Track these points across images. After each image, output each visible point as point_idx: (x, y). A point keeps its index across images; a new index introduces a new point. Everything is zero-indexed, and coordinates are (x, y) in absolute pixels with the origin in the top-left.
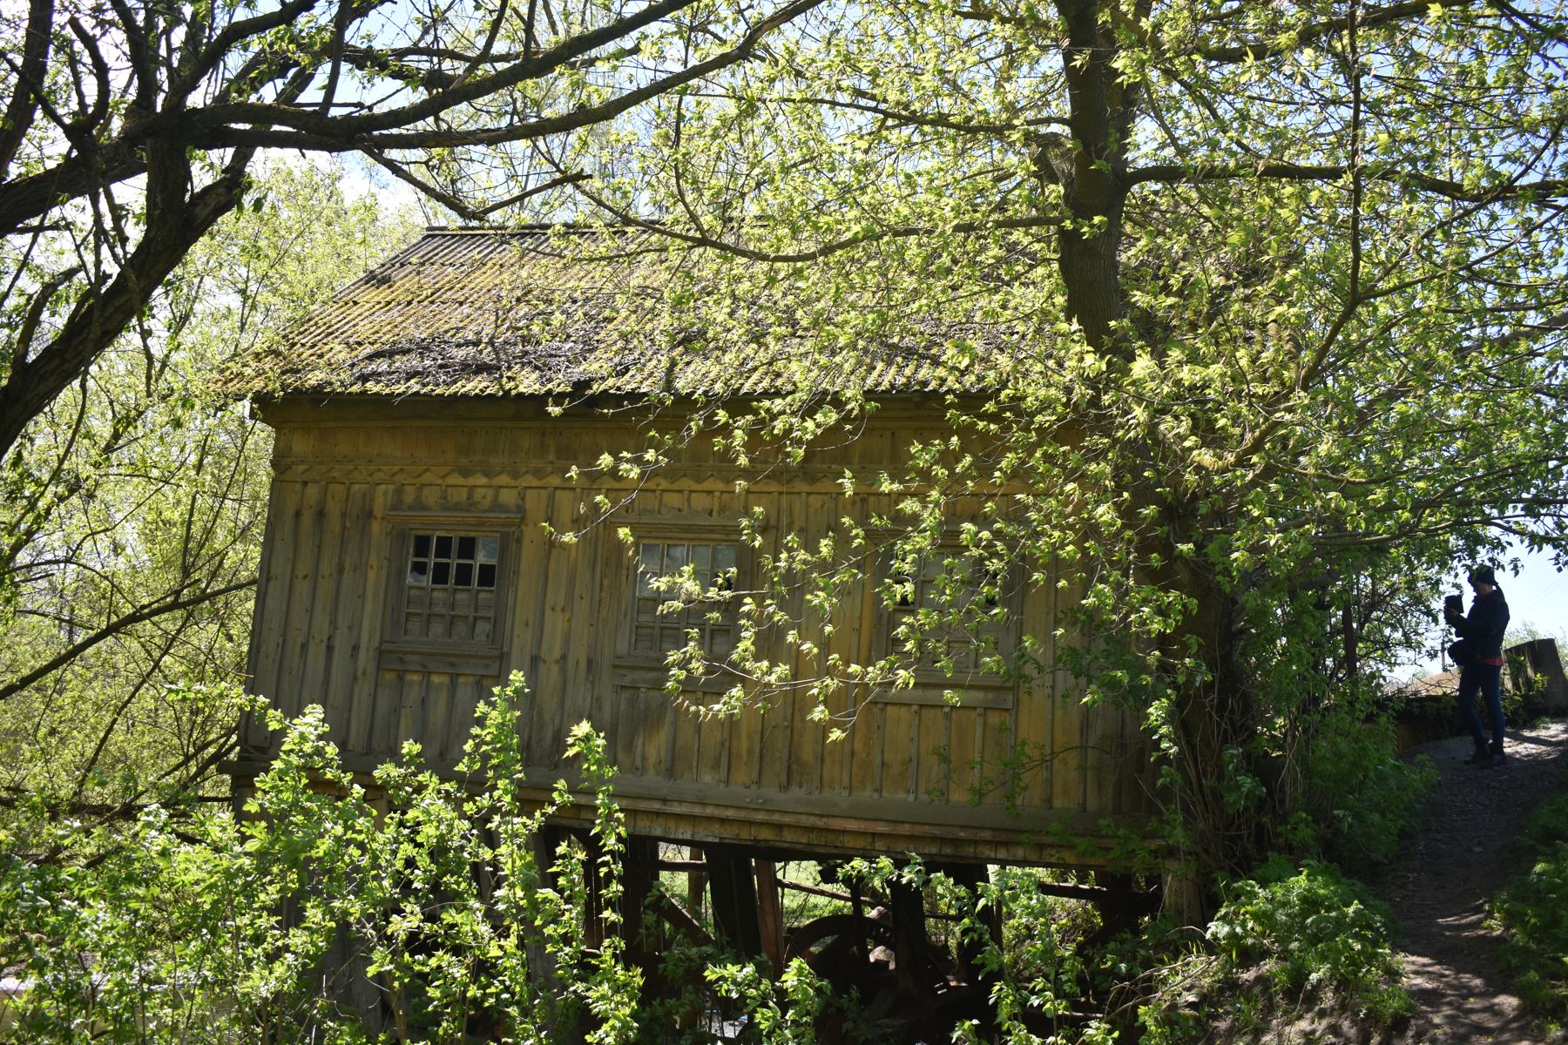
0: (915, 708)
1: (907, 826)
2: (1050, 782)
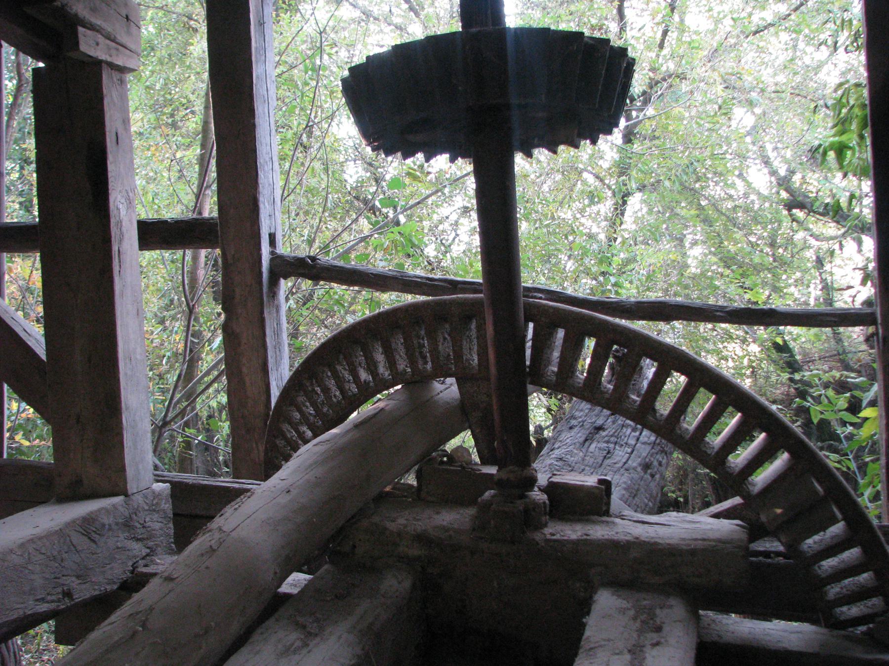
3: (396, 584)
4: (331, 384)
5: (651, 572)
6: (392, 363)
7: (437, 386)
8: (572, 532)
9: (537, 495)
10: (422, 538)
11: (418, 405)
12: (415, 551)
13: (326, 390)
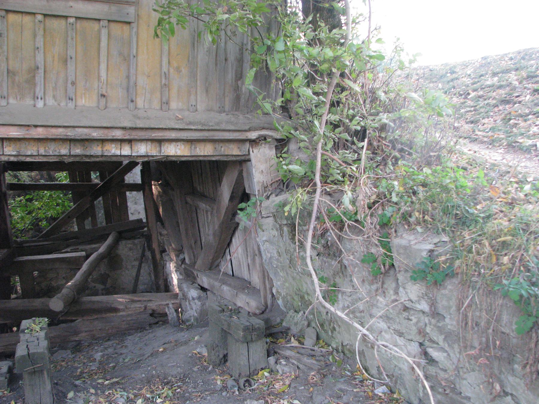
0: (40, 17)
1: (40, 130)
2: (166, 86)
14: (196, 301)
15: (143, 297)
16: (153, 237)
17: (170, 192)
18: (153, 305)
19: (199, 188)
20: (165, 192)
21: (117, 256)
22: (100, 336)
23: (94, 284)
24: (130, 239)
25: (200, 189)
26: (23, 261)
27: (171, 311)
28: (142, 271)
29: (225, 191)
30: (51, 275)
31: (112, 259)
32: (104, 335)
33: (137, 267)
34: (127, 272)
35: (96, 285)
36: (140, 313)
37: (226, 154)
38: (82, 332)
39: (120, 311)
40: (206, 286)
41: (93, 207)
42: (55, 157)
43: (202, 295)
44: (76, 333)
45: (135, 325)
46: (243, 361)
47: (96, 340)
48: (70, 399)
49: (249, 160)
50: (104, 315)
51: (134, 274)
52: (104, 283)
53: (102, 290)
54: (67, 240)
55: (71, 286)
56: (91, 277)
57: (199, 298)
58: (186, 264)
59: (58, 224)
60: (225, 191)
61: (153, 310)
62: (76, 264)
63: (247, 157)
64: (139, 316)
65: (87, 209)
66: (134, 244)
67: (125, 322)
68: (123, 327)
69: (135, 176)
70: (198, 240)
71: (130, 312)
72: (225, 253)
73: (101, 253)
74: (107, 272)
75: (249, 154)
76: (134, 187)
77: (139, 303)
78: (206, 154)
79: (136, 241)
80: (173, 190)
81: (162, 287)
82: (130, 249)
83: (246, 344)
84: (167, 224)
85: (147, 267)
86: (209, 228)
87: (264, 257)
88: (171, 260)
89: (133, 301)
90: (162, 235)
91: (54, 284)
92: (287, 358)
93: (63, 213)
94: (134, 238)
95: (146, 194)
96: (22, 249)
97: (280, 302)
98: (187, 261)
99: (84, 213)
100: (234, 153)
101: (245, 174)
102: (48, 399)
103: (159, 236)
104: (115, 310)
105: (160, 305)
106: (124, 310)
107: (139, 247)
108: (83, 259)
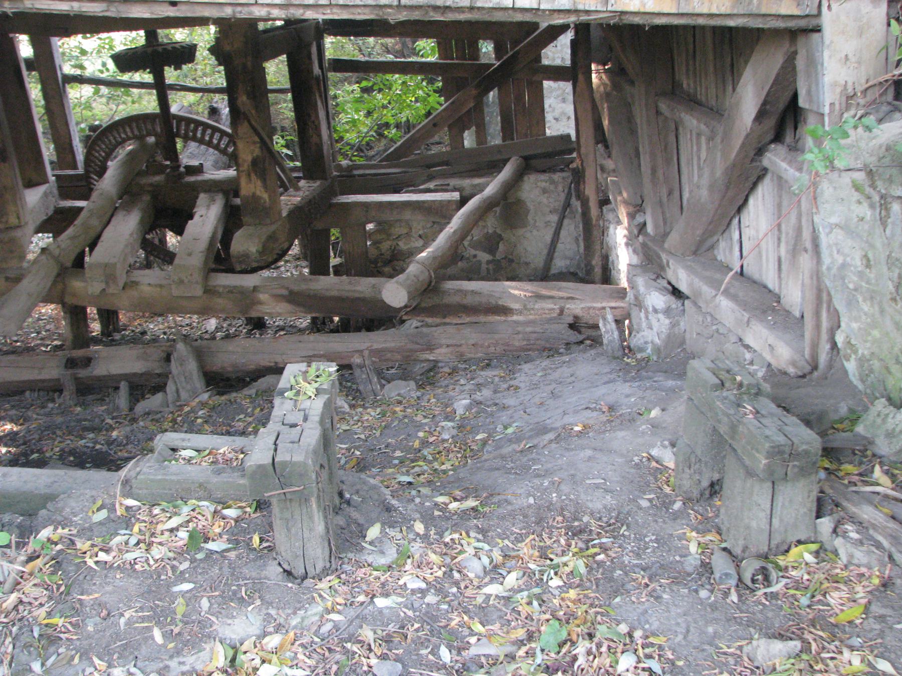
3: (147, 198)
4: (111, 138)
5: (213, 187)
6: (132, 132)
7: (148, 139)
8: (192, 179)
9: (182, 169)
10: (151, 185)
11: (144, 146)
12: (150, 189)
13: (110, 141)
14: (661, 316)
15: (559, 289)
16: (587, 174)
17: (628, 88)
18: (576, 308)
19: (686, 84)
20: (616, 86)
21: (519, 202)
22: (473, 356)
23: (473, 252)
24: (544, 171)
25: (688, 85)
26: (348, 203)
27: (608, 327)
28: (563, 233)
29: (748, 99)
30: (398, 230)
31: (508, 207)
32: (480, 355)
33: (554, 225)
34: (535, 232)
35: (477, 252)
36: (550, 321)
37: (763, 11)
38: (441, 346)
39: (513, 314)
40: (683, 287)
41: (479, 106)
42: (367, 10)
43: (674, 306)
44: (430, 348)
45: (538, 342)
46: (757, 520)
47: (465, 364)
48: (371, 543)
49: (817, 30)
50: (482, 318)
51: (548, 238)
52: (492, 250)
53: (488, 262)
54: (429, 167)
55: (427, 258)
56: (469, 238)
57: (667, 311)
58: (647, 235)
59: (417, 136)
60: (748, 99)
61: (576, 317)
62: (442, 213)
63: (813, 22)
64: (547, 326)
65: (469, 111)
66: (553, 182)
67: (521, 336)
68: (517, 344)
69: (558, 53)
70: (675, 190)
71: (531, 317)
72: (729, 224)
73: (489, 198)
74: (499, 231)
75: (819, 14)
76: (557, 73)
77: (550, 301)
78: (714, 11)
79: (557, 176)
80: (632, 83)
81: (598, 271)
82: (545, 191)
83: (770, 484)
84: (615, 152)
85: (572, 227)
86: (702, 168)
87: (826, 260)
88: (619, 222)
89: (539, 297)
90: (607, 171)
91: (403, 246)
92: (860, 524)
93: (429, 113)
94: (551, 170)
95: (578, 89)
96: (352, 181)
97: (851, 366)
98: (650, 229)
99: (460, 119)
100: (784, 11)
101: (800, 63)
102: (319, 551)
103: (599, 172)
104: (505, 311)
105: (589, 308)
106: (520, 313)
107: (560, 188)
108: (454, 207)
